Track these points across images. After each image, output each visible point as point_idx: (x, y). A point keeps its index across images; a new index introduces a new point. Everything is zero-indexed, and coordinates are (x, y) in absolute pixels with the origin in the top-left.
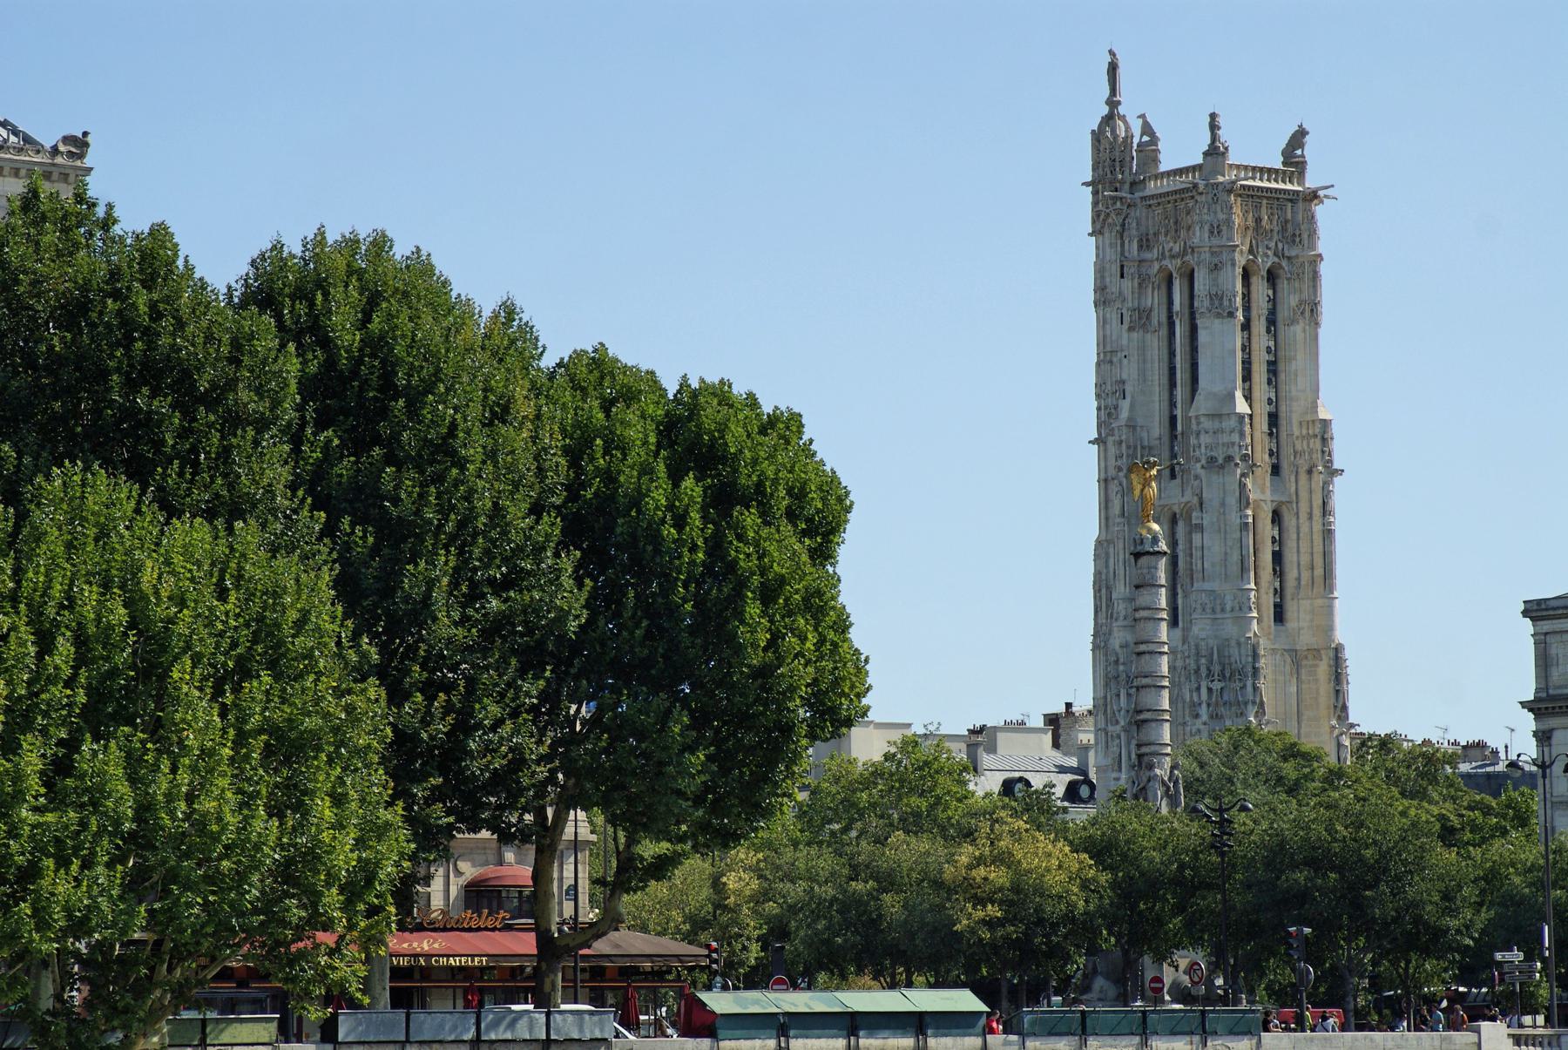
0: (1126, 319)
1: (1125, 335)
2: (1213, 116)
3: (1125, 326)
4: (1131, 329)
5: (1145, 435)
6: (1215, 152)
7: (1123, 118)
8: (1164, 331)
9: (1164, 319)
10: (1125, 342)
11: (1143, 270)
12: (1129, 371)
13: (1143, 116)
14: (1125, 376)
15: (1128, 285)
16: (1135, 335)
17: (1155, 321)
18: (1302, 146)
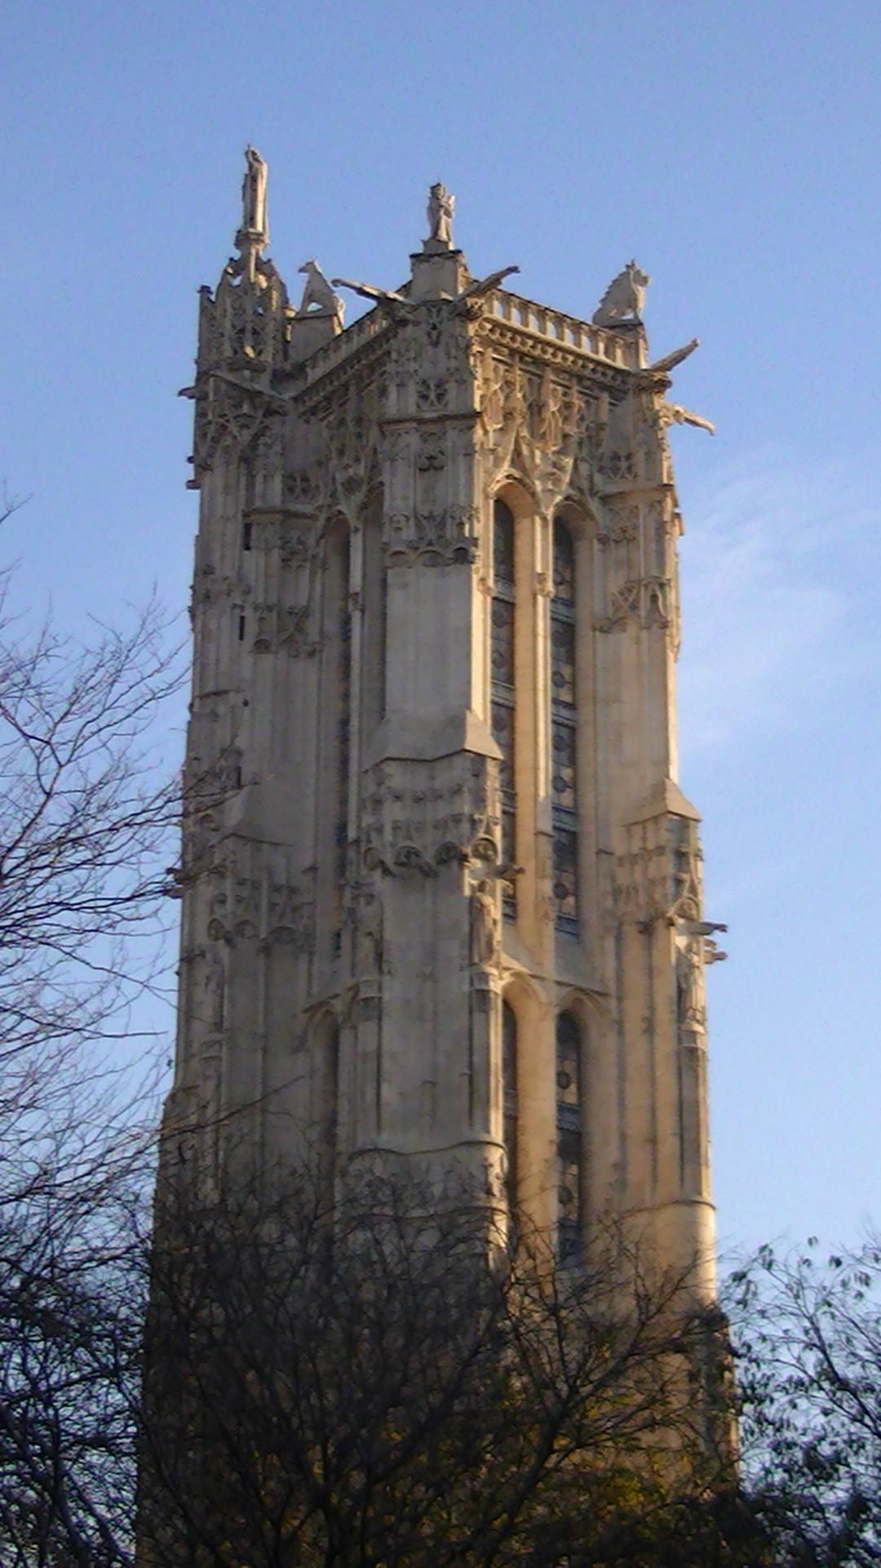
0: (252, 628)
1: (247, 661)
2: (435, 189)
3: (250, 639)
4: (261, 646)
5: (279, 862)
6: (435, 255)
7: (264, 267)
8: (332, 652)
9: (332, 626)
10: (246, 673)
11: (294, 535)
12: (253, 736)
13: (308, 268)
14: (241, 742)
15: (254, 563)
16: (267, 660)
17: (313, 634)
18: (632, 303)
